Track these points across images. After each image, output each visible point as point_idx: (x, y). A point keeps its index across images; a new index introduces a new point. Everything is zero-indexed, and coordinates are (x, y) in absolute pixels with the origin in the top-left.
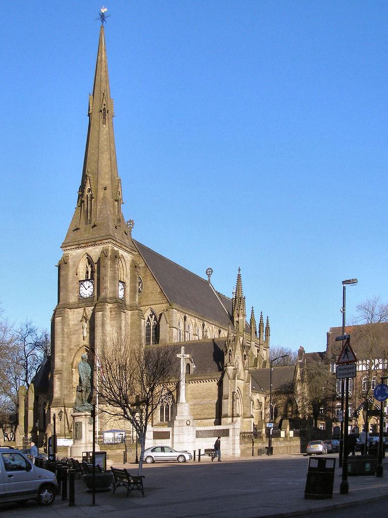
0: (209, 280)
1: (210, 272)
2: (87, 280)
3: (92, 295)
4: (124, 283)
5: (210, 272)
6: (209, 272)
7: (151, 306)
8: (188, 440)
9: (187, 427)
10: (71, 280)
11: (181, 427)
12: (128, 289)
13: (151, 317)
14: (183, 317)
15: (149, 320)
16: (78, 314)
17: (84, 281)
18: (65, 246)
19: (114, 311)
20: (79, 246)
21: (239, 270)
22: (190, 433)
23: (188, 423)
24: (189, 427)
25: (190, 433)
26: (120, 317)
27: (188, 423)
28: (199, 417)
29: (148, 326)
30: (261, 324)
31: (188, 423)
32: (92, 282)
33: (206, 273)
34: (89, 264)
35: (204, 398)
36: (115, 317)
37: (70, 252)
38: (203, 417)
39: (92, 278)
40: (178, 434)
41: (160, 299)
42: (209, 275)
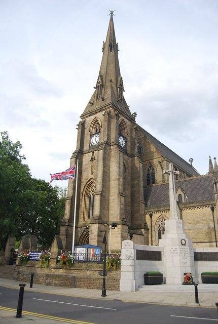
2: (97, 133)
4: (125, 138)
6: (191, 160)
9: (183, 247)
12: (129, 144)
15: (148, 170)
16: (89, 156)
18: (82, 117)
20: (91, 114)
22: (186, 255)
28: (195, 241)
29: (148, 174)
31: (184, 243)
35: (198, 223)
38: (198, 240)
39: (100, 132)
42: (191, 162)
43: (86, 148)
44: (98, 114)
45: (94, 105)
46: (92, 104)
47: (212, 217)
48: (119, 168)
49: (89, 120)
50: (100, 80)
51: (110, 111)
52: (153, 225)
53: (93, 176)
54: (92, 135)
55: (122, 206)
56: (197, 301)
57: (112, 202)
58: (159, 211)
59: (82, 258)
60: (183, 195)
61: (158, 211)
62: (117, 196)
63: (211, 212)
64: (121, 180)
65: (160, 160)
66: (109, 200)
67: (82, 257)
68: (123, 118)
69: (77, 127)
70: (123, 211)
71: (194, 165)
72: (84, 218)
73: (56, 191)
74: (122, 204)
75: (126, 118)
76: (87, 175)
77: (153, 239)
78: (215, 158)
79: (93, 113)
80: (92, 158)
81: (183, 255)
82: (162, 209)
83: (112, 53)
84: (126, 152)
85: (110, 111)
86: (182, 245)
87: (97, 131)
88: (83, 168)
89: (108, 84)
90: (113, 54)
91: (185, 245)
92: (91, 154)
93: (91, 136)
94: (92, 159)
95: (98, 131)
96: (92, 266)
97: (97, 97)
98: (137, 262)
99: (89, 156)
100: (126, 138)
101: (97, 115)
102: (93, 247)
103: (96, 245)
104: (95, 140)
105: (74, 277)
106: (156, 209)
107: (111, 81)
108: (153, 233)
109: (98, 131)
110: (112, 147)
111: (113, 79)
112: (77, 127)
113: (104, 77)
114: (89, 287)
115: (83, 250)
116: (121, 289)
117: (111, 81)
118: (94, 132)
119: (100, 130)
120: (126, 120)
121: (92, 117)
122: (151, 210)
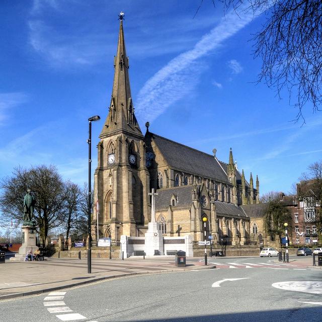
6: (215, 151)
17: (111, 154)
27: (156, 235)
30: (251, 180)
31: (156, 235)
43: (105, 165)
44: (113, 137)
45: (109, 127)
46: (108, 126)
48: (129, 183)
49: (106, 140)
50: (112, 104)
51: (121, 137)
53: (111, 188)
55: (132, 211)
60: (175, 200)
62: (127, 204)
64: (131, 192)
65: (166, 168)
66: (122, 207)
70: (132, 214)
76: (106, 188)
80: (110, 174)
83: (123, 72)
85: (121, 137)
88: (104, 181)
89: (120, 107)
90: (124, 73)
92: (109, 171)
94: (110, 175)
97: (111, 120)
98: (128, 245)
104: (112, 159)
107: (122, 105)
110: (123, 167)
113: (116, 99)
117: (122, 105)
118: (110, 152)
121: (108, 139)
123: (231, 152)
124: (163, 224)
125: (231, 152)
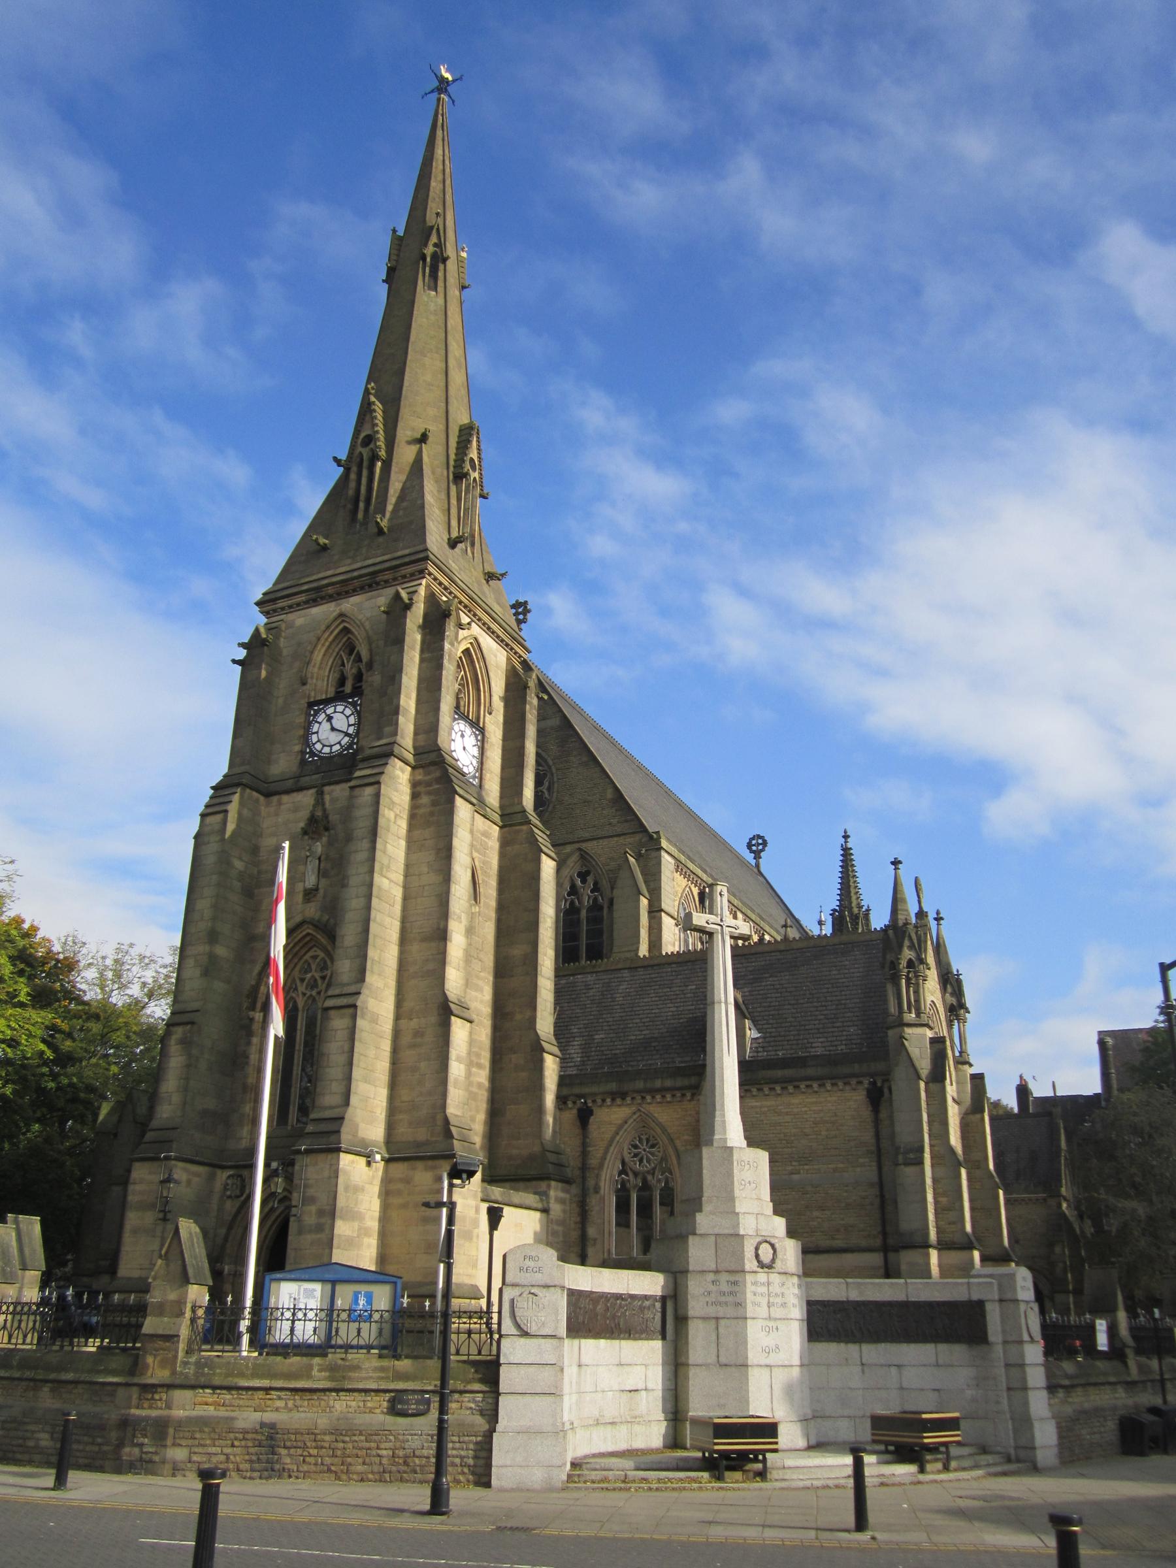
0: (757, 866)
1: (759, 844)
3: (350, 746)
5: (759, 844)
6: (757, 845)
7: (584, 846)
8: (767, 1351)
9: (762, 1277)
10: (280, 701)
11: (724, 1277)
13: (584, 881)
14: (696, 891)
16: (296, 810)
17: (327, 702)
18: (267, 603)
19: (429, 793)
20: (317, 596)
21: (846, 837)
23: (766, 1253)
24: (775, 1278)
25: (777, 1312)
26: (450, 812)
31: (766, 1253)
32: (354, 704)
33: (749, 846)
34: (350, 654)
36: (432, 814)
37: (291, 617)
39: (358, 691)
40: (712, 1311)
41: (614, 821)
42: (757, 855)
44: (355, 599)
47: (868, 1136)
52: (593, 1162)
54: (315, 705)
56: (861, 1523)
57: (413, 1046)
58: (623, 1096)
59: (307, 1331)
61: (619, 1096)
63: (866, 1113)
67: (310, 1326)
68: (476, 630)
69: (242, 654)
71: (1040, 1090)
72: (1008, 1301)
73: (69, 965)
74: (459, 1059)
75: (489, 631)
77: (591, 1232)
78: (896, 863)
79: (330, 590)
80: (312, 820)
81: (763, 1311)
82: (640, 1085)
84: (481, 800)
86: (762, 1265)
87: (342, 681)
91: (770, 1266)
92: (306, 799)
93: (311, 705)
94: (316, 826)
95: (348, 688)
96: (357, 1368)
99: (296, 810)
100: (482, 731)
101: (350, 605)
102: (356, 1276)
103: (373, 1268)
105: (272, 1426)
106: (613, 1086)
108: (593, 1201)
109: (348, 688)
111: (436, 429)
112: (242, 654)
114: (340, 1472)
115: (309, 1294)
116: (494, 1482)
119: (359, 677)
120: (487, 642)
121: (323, 612)
122: (586, 1090)
123: (846, 853)
124: (646, 1187)
125: (846, 853)
